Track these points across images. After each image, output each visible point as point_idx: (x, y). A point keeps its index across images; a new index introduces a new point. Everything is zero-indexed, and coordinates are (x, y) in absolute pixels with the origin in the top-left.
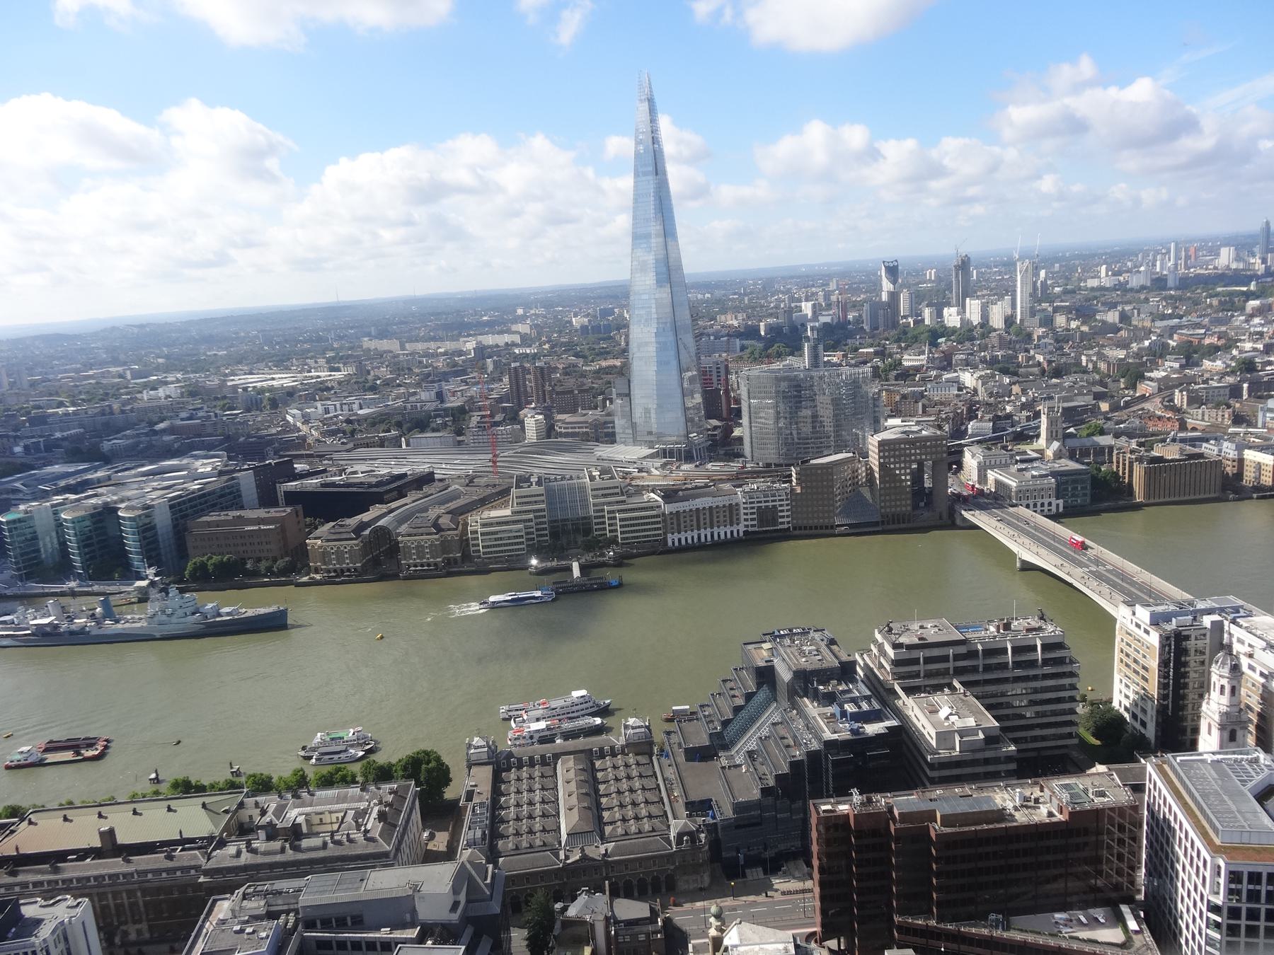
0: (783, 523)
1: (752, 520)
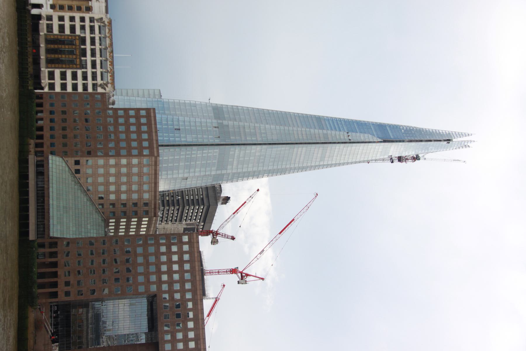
0: (51, 76)
1: (62, 28)
